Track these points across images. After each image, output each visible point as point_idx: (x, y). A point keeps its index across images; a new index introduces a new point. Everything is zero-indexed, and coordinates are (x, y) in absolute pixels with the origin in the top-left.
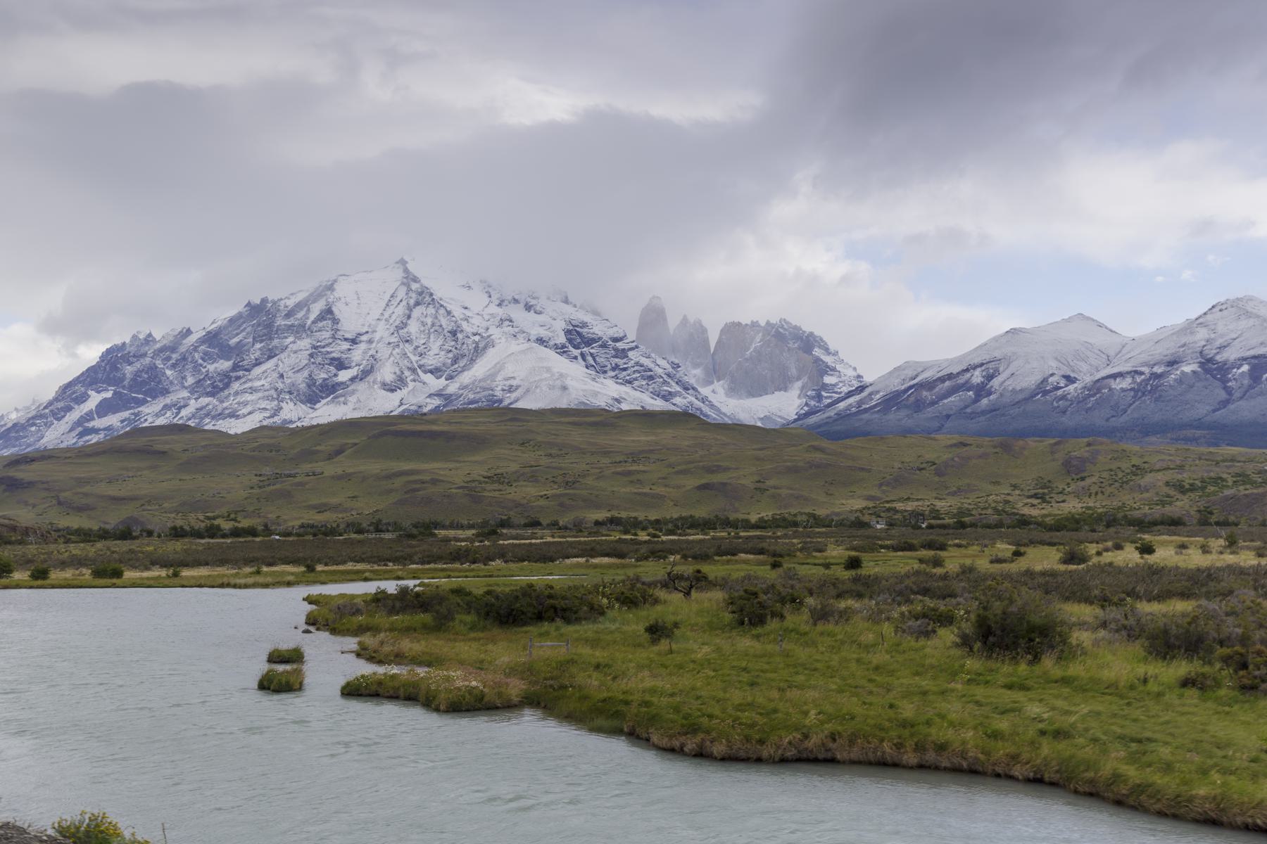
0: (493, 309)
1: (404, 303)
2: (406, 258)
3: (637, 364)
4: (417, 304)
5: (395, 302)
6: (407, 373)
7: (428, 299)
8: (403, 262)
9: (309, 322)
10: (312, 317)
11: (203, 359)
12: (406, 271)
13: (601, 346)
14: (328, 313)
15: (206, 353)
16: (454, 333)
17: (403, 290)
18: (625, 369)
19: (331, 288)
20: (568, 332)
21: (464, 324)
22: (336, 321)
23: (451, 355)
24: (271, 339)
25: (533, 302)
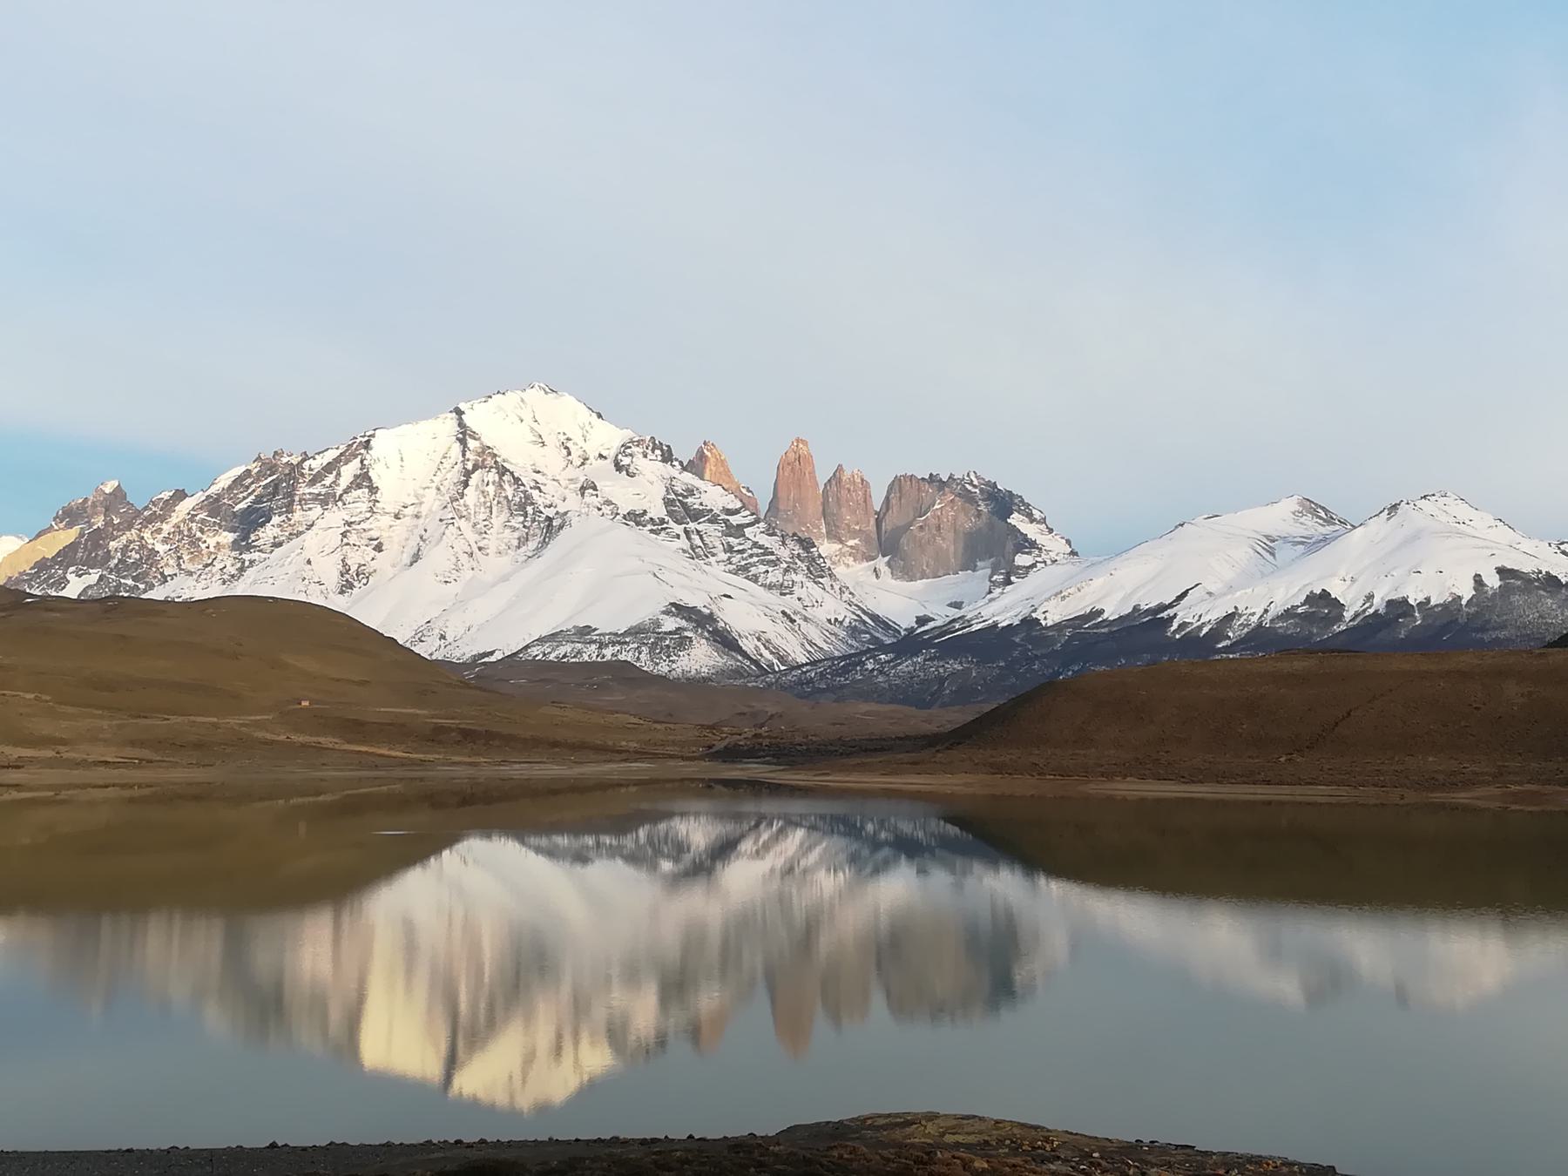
0: (572, 472)
1: (460, 466)
2: (462, 406)
3: (755, 544)
4: (476, 467)
5: (447, 464)
6: (464, 558)
7: (490, 462)
8: (459, 412)
9: (339, 491)
10: (344, 482)
11: (202, 531)
12: (461, 424)
13: (710, 521)
14: (363, 480)
15: (203, 521)
16: (522, 507)
17: (457, 447)
18: (739, 552)
19: (367, 445)
20: (668, 503)
21: (535, 493)
22: (373, 490)
23: (516, 534)
24: (290, 511)
25: (626, 461)
